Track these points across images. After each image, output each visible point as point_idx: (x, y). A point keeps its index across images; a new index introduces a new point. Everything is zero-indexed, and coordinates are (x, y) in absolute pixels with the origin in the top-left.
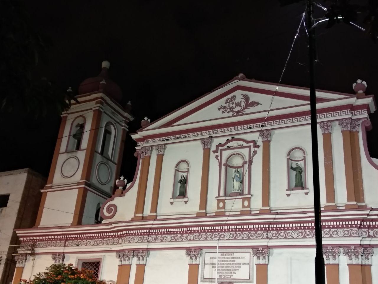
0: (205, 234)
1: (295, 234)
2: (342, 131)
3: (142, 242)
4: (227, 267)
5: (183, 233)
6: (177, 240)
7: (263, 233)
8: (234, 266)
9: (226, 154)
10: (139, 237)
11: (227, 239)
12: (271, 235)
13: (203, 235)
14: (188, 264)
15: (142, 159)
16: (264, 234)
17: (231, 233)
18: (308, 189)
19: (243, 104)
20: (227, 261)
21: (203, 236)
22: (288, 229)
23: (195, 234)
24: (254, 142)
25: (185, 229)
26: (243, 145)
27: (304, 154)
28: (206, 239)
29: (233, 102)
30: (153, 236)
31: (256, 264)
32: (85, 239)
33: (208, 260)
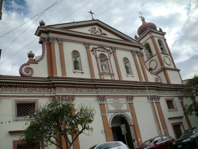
2: (138, 56)
4: (118, 105)
5: (93, 88)
8: (121, 104)
9: (98, 53)
14: (100, 104)
15: (46, 44)
19: (100, 32)
20: (117, 102)
23: (100, 89)
24: (109, 50)
25: (94, 86)
27: (128, 60)
31: (129, 104)
32: (19, 87)
33: (108, 102)
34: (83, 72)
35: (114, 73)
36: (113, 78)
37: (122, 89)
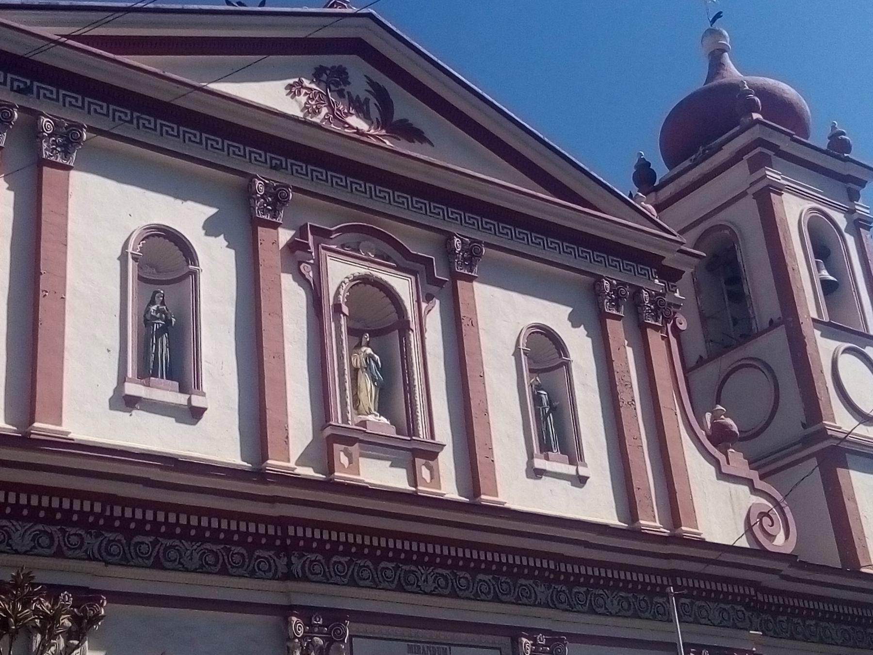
0: (349, 563)
1: (612, 601)
2: (642, 328)
3: (59, 554)
6: (231, 570)
7: (534, 586)
10: (40, 527)
11: (427, 590)
12: (552, 596)
13: (340, 562)
16: (536, 588)
17: (440, 571)
18: (585, 465)
19: (375, 113)
21: (340, 566)
22: (596, 586)
23: (312, 557)
26: (388, 259)
28: (353, 583)
29: (340, 87)
30: (111, 536)
34: (205, 409)
35: (438, 439)
36: (425, 473)
37: (487, 571)
